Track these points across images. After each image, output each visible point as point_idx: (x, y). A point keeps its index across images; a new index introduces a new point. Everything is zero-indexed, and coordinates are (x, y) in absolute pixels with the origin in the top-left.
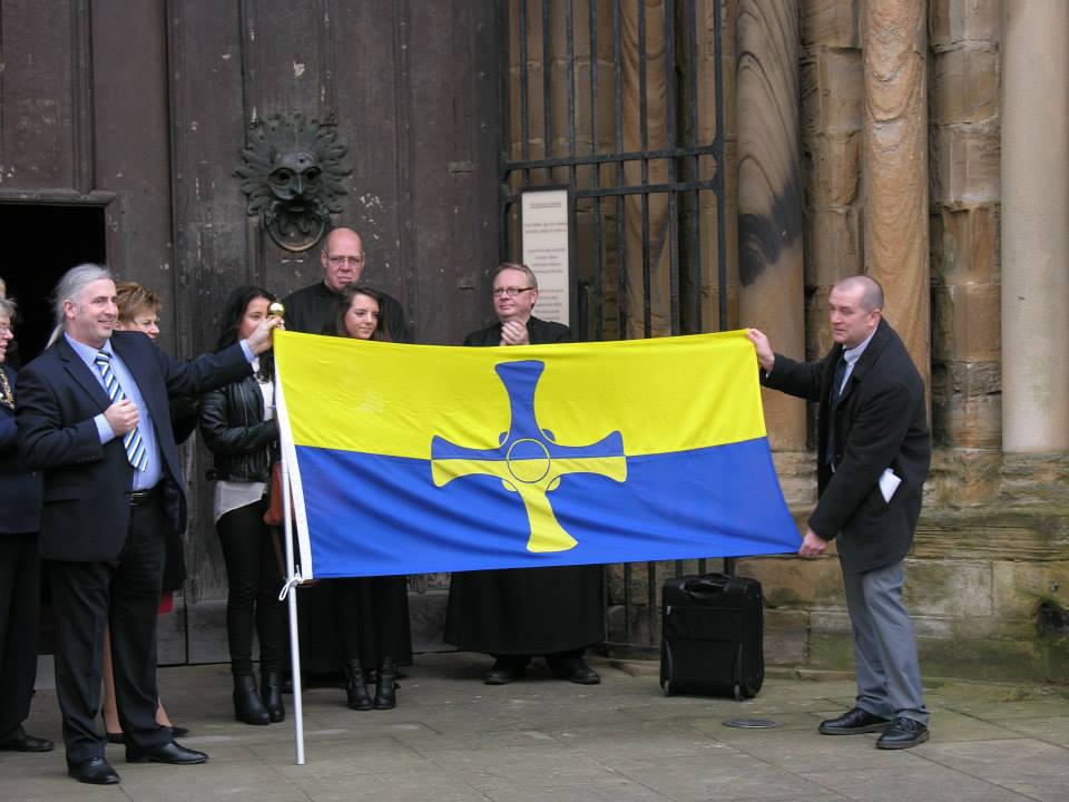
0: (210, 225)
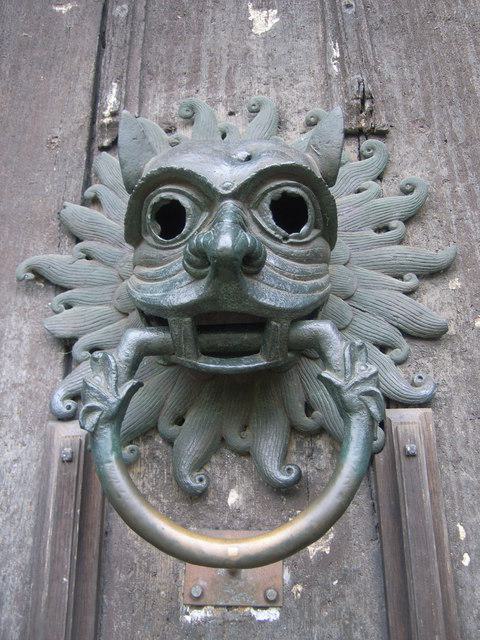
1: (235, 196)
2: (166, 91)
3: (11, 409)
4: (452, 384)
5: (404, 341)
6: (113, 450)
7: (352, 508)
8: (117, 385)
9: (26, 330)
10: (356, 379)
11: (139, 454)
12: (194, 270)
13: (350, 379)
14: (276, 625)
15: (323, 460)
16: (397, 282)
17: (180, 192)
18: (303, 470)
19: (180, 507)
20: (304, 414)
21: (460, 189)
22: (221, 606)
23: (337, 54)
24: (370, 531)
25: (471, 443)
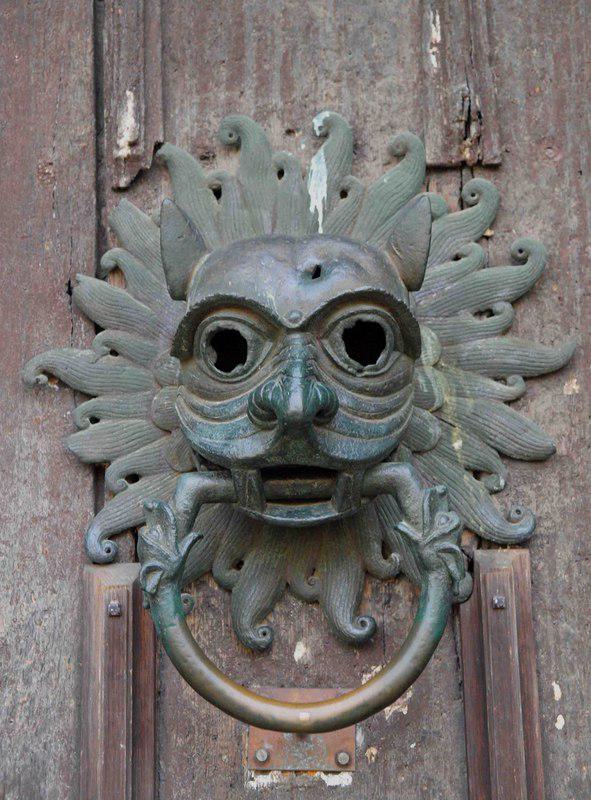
1: (302, 329)
3: (35, 549)
5: (499, 461)
7: (433, 663)
8: (179, 539)
9: (43, 446)
10: (435, 534)
12: (259, 422)
14: (349, 790)
15: (402, 609)
16: (498, 386)
17: (240, 321)
18: (379, 620)
19: (242, 663)
20: (380, 556)
22: (290, 771)
23: (436, 36)
24: (453, 690)
25: (575, 589)
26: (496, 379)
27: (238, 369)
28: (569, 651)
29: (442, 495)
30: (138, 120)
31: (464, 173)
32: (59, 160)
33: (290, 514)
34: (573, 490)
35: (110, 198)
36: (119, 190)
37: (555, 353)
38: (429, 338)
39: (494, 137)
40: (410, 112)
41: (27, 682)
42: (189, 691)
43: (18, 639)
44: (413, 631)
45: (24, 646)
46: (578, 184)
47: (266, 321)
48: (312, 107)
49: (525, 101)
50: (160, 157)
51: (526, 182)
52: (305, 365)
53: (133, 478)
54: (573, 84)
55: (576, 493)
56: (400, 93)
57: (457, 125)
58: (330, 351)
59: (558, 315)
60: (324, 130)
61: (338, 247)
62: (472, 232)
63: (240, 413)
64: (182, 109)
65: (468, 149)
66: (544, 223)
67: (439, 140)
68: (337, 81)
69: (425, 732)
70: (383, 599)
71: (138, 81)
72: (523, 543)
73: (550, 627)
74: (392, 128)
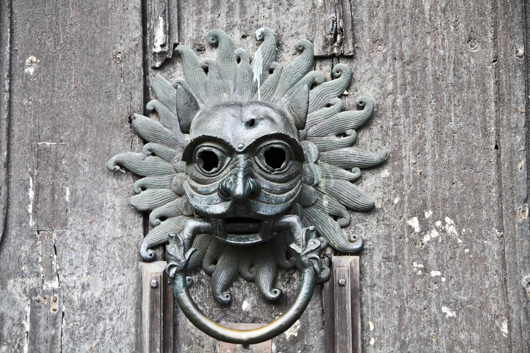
0: (55, 284)
2: (196, 14)
3: (114, 254)
4: (375, 241)
5: (346, 212)
6: (183, 287)
8: (185, 252)
9: (118, 201)
10: (308, 250)
11: (193, 281)
13: (305, 250)
16: (348, 173)
18: (284, 290)
19: (216, 311)
20: (285, 259)
21: (399, 101)
24: (320, 325)
25: (382, 276)
26: (347, 169)
27: (214, 170)
28: (379, 306)
29: (312, 231)
30: (165, 33)
31: (334, 60)
32: (124, 51)
33: (239, 240)
34: (383, 226)
35: (151, 72)
36: (155, 68)
37: (376, 157)
38: (313, 149)
39: (350, 41)
40: (307, 26)
41: (111, 319)
42: (190, 324)
43: (106, 298)
44: (296, 298)
45: (109, 302)
46: (394, 65)
47: (227, 147)
48: (256, 23)
49: (368, 19)
50: (177, 51)
51: (367, 64)
52: (244, 171)
53: (163, 218)
54: (394, 9)
55: (385, 228)
56: (302, 15)
57: (330, 36)
58: (258, 162)
59: (380, 136)
60: (261, 38)
61: (263, 110)
62: (336, 92)
63: (214, 192)
64: (188, 24)
65: (336, 48)
66: (375, 86)
67: (321, 43)
68: (269, 8)
69: (305, 345)
70: (287, 280)
71: (165, 11)
72: (359, 252)
73: (369, 295)
74: (298, 34)
